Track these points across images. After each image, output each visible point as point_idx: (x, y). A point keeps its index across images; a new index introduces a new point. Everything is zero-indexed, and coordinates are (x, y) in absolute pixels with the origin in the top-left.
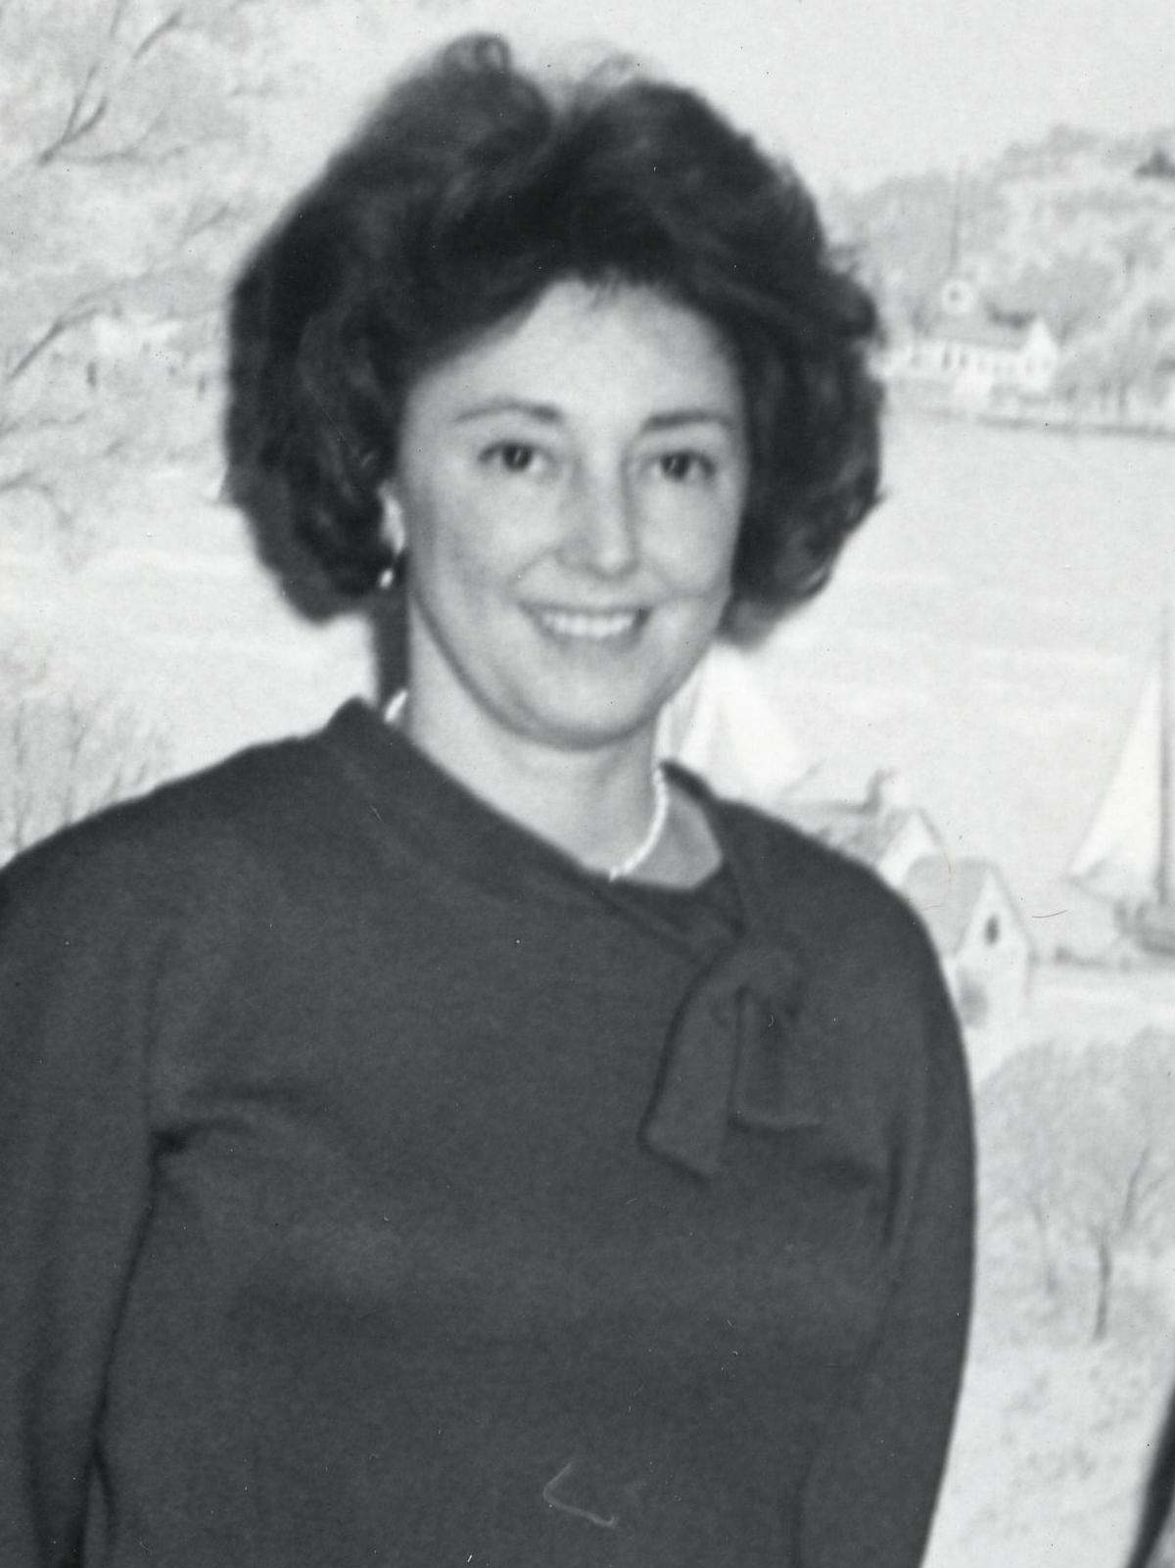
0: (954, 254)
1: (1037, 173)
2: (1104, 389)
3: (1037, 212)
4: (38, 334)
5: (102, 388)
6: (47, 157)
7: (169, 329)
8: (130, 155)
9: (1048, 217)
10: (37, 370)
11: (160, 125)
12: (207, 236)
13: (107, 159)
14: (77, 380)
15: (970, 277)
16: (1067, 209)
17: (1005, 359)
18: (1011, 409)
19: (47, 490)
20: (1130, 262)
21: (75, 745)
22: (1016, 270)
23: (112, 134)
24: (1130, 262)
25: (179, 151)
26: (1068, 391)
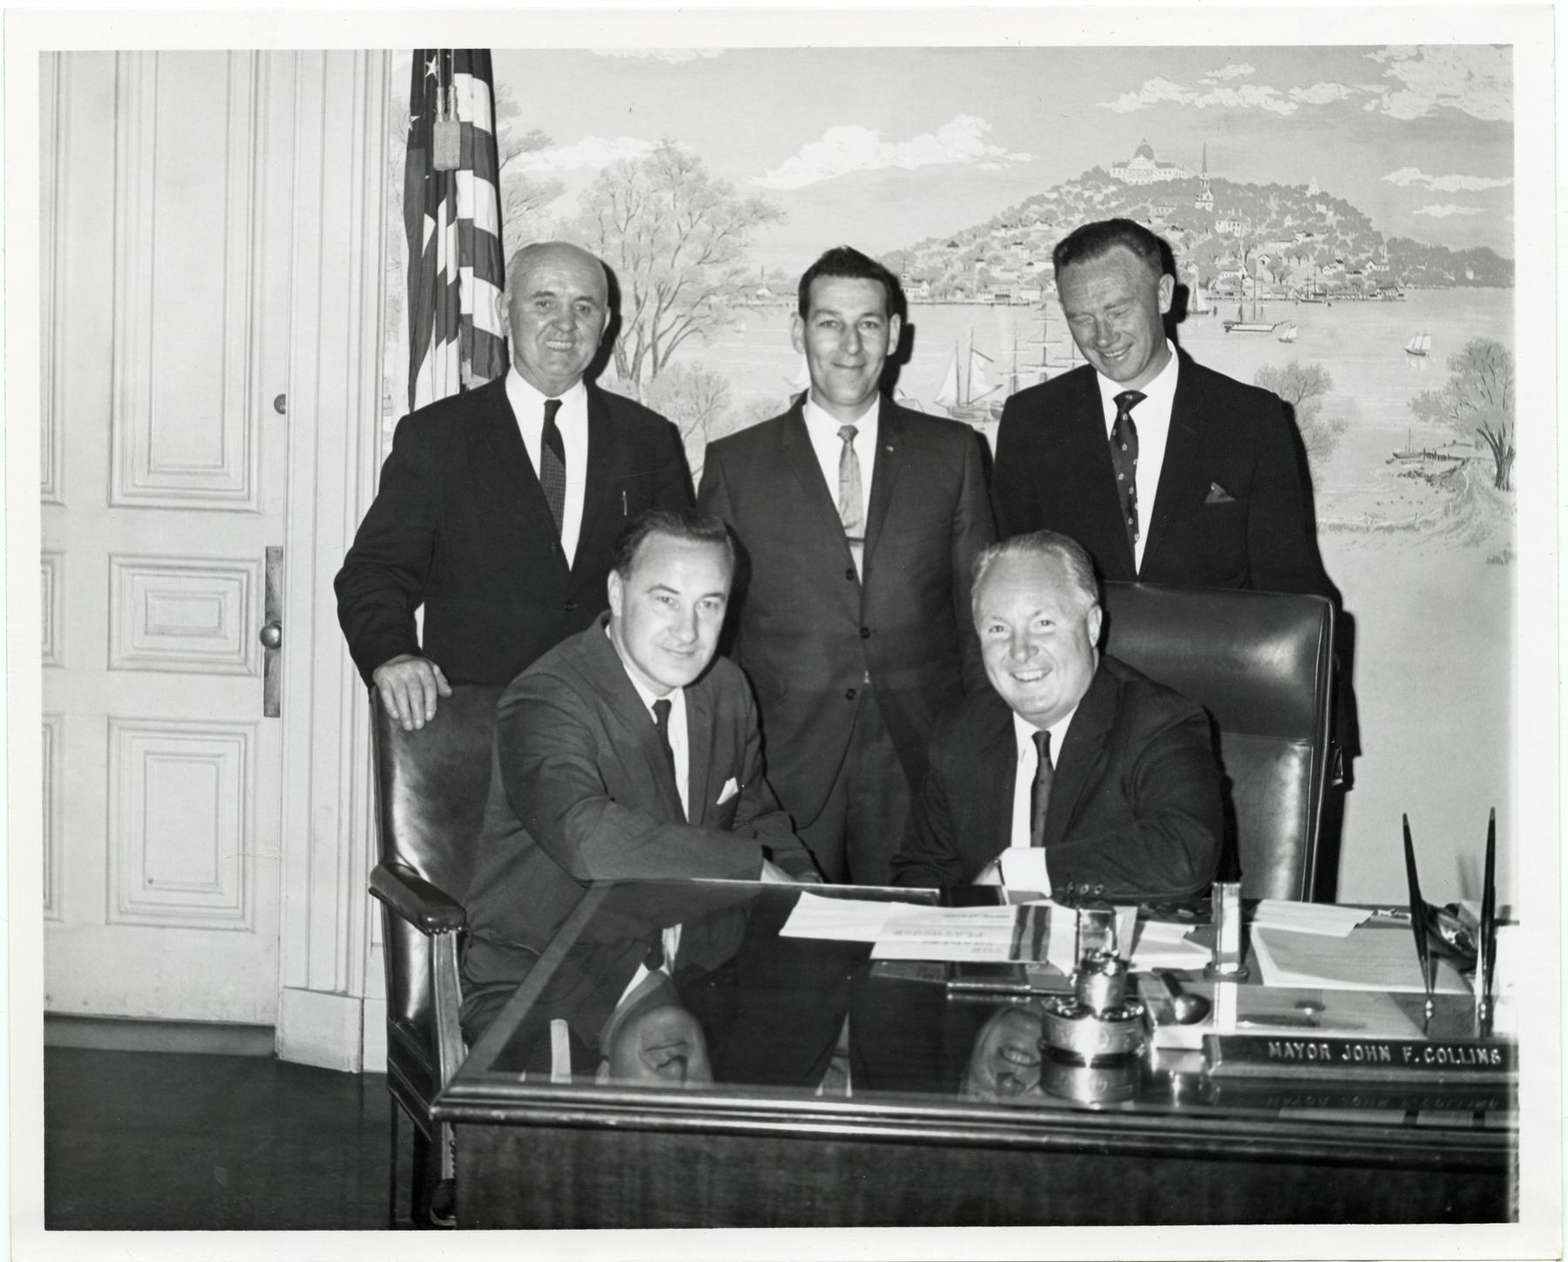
0: (904, 268)
1: (923, 248)
2: (941, 295)
3: (924, 255)
4: (698, 299)
5: (713, 310)
6: (699, 263)
7: (725, 297)
8: (716, 261)
9: (926, 258)
10: (698, 307)
11: (723, 254)
12: (734, 277)
13: (712, 262)
14: (707, 308)
15: (908, 272)
16: (931, 256)
17: (916, 289)
18: (919, 301)
19: (701, 331)
20: (946, 266)
21: (708, 383)
22: (918, 270)
23: (712, 257)
24: (946, 266)
25: (727, 260)
26: (932, 296)
